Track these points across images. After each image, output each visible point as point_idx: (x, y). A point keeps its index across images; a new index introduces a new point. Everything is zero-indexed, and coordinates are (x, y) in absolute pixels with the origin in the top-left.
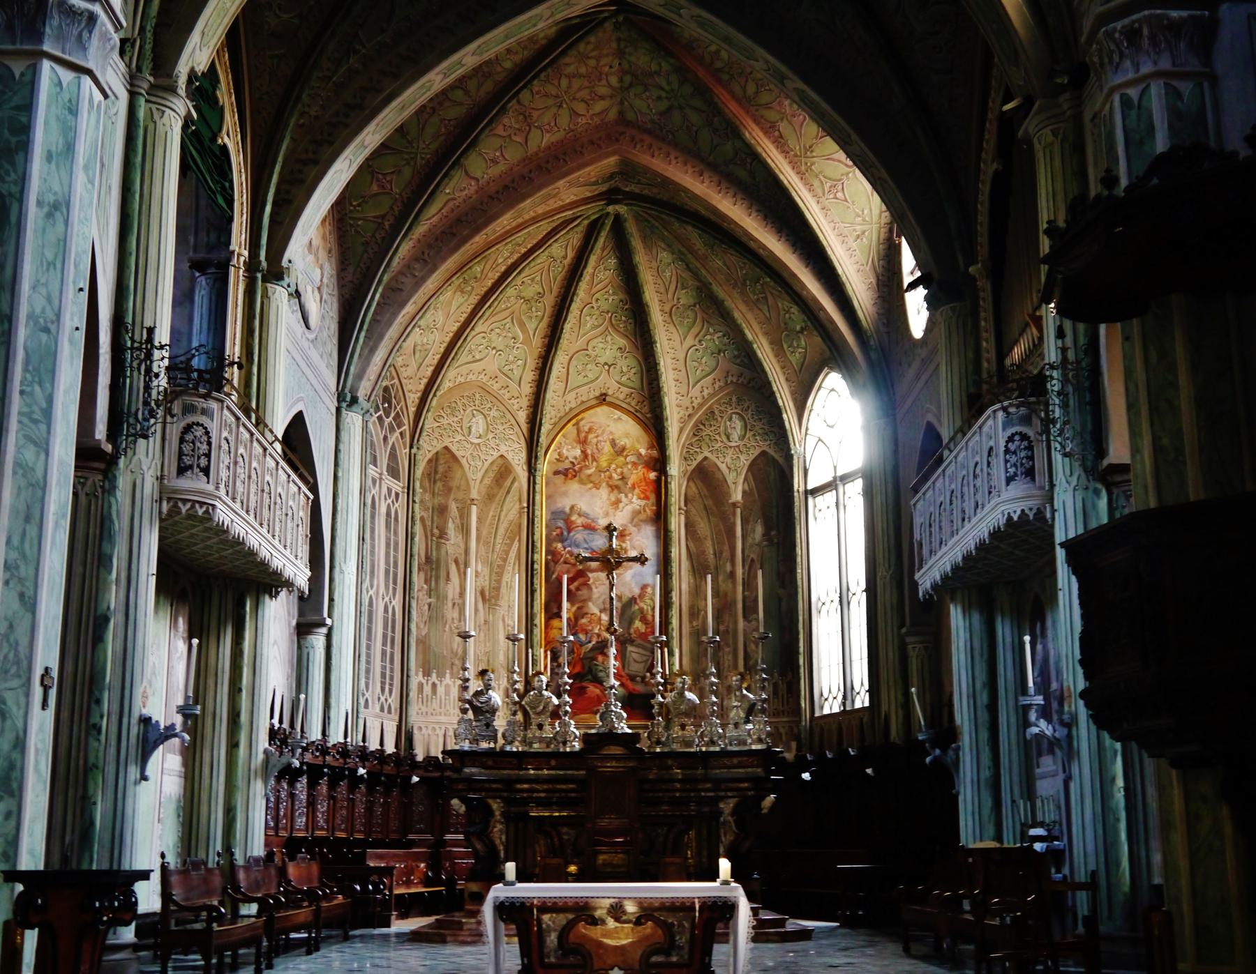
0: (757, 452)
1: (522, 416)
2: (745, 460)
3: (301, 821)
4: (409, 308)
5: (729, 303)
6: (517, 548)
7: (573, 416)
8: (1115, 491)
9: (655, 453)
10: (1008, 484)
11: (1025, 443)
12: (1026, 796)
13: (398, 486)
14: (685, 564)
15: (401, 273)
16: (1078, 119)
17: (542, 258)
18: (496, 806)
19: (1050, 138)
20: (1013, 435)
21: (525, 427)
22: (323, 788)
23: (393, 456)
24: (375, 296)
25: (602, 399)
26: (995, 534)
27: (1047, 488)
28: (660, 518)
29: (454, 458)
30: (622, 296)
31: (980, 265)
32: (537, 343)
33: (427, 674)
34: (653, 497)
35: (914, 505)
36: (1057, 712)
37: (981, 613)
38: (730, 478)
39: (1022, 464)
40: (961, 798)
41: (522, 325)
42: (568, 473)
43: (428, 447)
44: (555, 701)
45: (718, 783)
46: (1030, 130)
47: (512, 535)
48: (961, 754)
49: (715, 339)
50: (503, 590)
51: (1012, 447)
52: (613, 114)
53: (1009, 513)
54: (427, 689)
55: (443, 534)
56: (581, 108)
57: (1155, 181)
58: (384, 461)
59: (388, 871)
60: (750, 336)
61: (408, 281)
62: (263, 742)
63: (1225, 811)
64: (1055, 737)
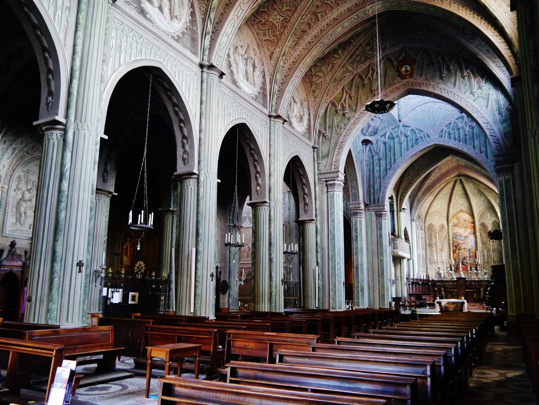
0: (493, 220)
1: (445, 215)
2: (491, 222)
3: (411, 291)
4: (422, 203)
5: (484, 193)
6: (446, 240)
7: (455, 215)
9: (473, 221)
13: (423, 232)
14: (480, 242)
15: (420, 197)
17: (446, 188)
18: (442, 289)
21: (446, 217)
22: (414, 285)
23: (421, 227)
24: (416, 202)
25: (461, 211)
28: (475, 233)
29: (433, 225)
30: (463, 192)
32: (447, 202)
33: (431, 265)
34: (473, 229)
38: (488, 225)
41: (443, 199)
42: (455, 225)
43: (428, 224)
44: (451, 272)
45: (480, 285)
47: (445, 238)
49: (483, 198)
50: (444, 248)
52: (456, 165)
54: (431, 267)
55: (432, 239)
56: (450, 165)
58: (420, 228)
59: (426, 299)
60: (489, 198)
61: (421, 199)
62: (405, 280)
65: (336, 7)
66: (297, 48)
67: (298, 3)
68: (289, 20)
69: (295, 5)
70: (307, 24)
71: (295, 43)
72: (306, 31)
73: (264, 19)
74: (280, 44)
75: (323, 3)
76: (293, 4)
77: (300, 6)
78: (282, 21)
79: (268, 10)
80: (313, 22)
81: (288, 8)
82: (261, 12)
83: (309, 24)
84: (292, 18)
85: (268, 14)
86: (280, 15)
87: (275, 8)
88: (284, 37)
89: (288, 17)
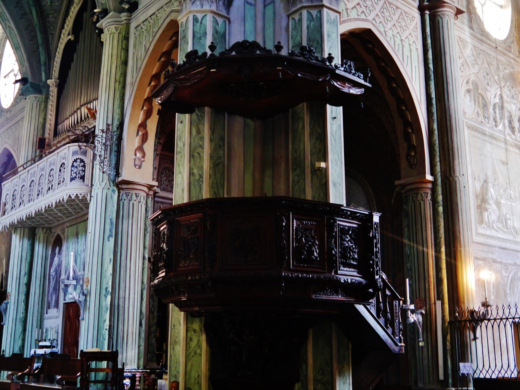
8: (122, 192)
10: (71, 181)
11: (82, 164)
12: (39, 327)
16: (128, 25)
19: (114, 30)
20: (77, 159)
26: (59, 204)
27: (90, 186)
31: (53, 80)
35: (4, 185)
36: (63, 289)
37: (29, 239)
39: (79, 173)
40: (4, 327)
46: (104, 25)
48: (9, 306)
51: (75, 164)
53: (70, 195)
57: (234, 53)
63: (204, 337)
64: (79, 300)
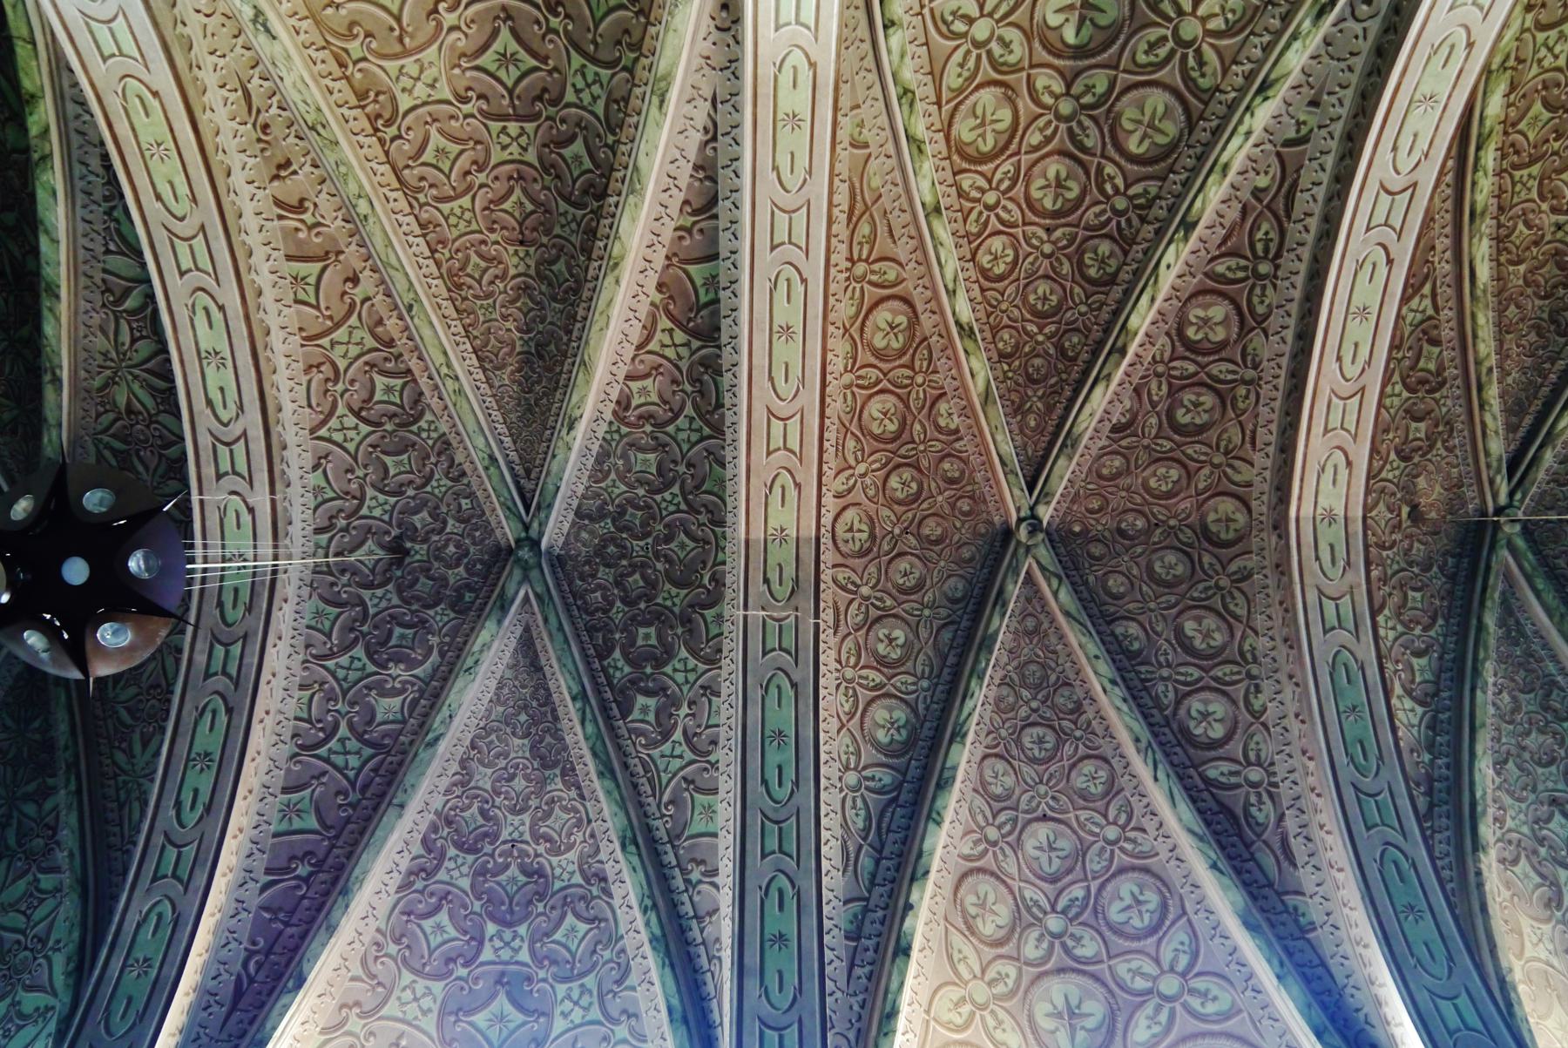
65: (305, 354)
66: (233, 97)
67: (421, 206)
68: (376, 130)
69: (420, 190)
70: (302, 201)
71: (254, 98)
72: (276, 177)
73: (452, 29)
74: (305, 24)
75: (352, 306)
76: (431, 186)
77: (407, 210)
78: (393, 99)
79: (477, 68)
80: (297, 230)
81: (428, 156)
82: (495, 33)
83: (300, 207)
84: (378, 150)
85: (464, 55)
86: (425, 104)
87: (465, 100)
88: (320, 66)
89: (393, 131)
